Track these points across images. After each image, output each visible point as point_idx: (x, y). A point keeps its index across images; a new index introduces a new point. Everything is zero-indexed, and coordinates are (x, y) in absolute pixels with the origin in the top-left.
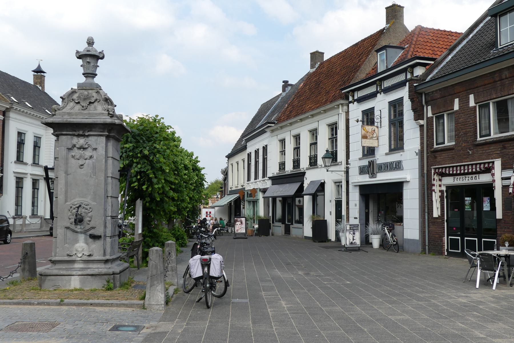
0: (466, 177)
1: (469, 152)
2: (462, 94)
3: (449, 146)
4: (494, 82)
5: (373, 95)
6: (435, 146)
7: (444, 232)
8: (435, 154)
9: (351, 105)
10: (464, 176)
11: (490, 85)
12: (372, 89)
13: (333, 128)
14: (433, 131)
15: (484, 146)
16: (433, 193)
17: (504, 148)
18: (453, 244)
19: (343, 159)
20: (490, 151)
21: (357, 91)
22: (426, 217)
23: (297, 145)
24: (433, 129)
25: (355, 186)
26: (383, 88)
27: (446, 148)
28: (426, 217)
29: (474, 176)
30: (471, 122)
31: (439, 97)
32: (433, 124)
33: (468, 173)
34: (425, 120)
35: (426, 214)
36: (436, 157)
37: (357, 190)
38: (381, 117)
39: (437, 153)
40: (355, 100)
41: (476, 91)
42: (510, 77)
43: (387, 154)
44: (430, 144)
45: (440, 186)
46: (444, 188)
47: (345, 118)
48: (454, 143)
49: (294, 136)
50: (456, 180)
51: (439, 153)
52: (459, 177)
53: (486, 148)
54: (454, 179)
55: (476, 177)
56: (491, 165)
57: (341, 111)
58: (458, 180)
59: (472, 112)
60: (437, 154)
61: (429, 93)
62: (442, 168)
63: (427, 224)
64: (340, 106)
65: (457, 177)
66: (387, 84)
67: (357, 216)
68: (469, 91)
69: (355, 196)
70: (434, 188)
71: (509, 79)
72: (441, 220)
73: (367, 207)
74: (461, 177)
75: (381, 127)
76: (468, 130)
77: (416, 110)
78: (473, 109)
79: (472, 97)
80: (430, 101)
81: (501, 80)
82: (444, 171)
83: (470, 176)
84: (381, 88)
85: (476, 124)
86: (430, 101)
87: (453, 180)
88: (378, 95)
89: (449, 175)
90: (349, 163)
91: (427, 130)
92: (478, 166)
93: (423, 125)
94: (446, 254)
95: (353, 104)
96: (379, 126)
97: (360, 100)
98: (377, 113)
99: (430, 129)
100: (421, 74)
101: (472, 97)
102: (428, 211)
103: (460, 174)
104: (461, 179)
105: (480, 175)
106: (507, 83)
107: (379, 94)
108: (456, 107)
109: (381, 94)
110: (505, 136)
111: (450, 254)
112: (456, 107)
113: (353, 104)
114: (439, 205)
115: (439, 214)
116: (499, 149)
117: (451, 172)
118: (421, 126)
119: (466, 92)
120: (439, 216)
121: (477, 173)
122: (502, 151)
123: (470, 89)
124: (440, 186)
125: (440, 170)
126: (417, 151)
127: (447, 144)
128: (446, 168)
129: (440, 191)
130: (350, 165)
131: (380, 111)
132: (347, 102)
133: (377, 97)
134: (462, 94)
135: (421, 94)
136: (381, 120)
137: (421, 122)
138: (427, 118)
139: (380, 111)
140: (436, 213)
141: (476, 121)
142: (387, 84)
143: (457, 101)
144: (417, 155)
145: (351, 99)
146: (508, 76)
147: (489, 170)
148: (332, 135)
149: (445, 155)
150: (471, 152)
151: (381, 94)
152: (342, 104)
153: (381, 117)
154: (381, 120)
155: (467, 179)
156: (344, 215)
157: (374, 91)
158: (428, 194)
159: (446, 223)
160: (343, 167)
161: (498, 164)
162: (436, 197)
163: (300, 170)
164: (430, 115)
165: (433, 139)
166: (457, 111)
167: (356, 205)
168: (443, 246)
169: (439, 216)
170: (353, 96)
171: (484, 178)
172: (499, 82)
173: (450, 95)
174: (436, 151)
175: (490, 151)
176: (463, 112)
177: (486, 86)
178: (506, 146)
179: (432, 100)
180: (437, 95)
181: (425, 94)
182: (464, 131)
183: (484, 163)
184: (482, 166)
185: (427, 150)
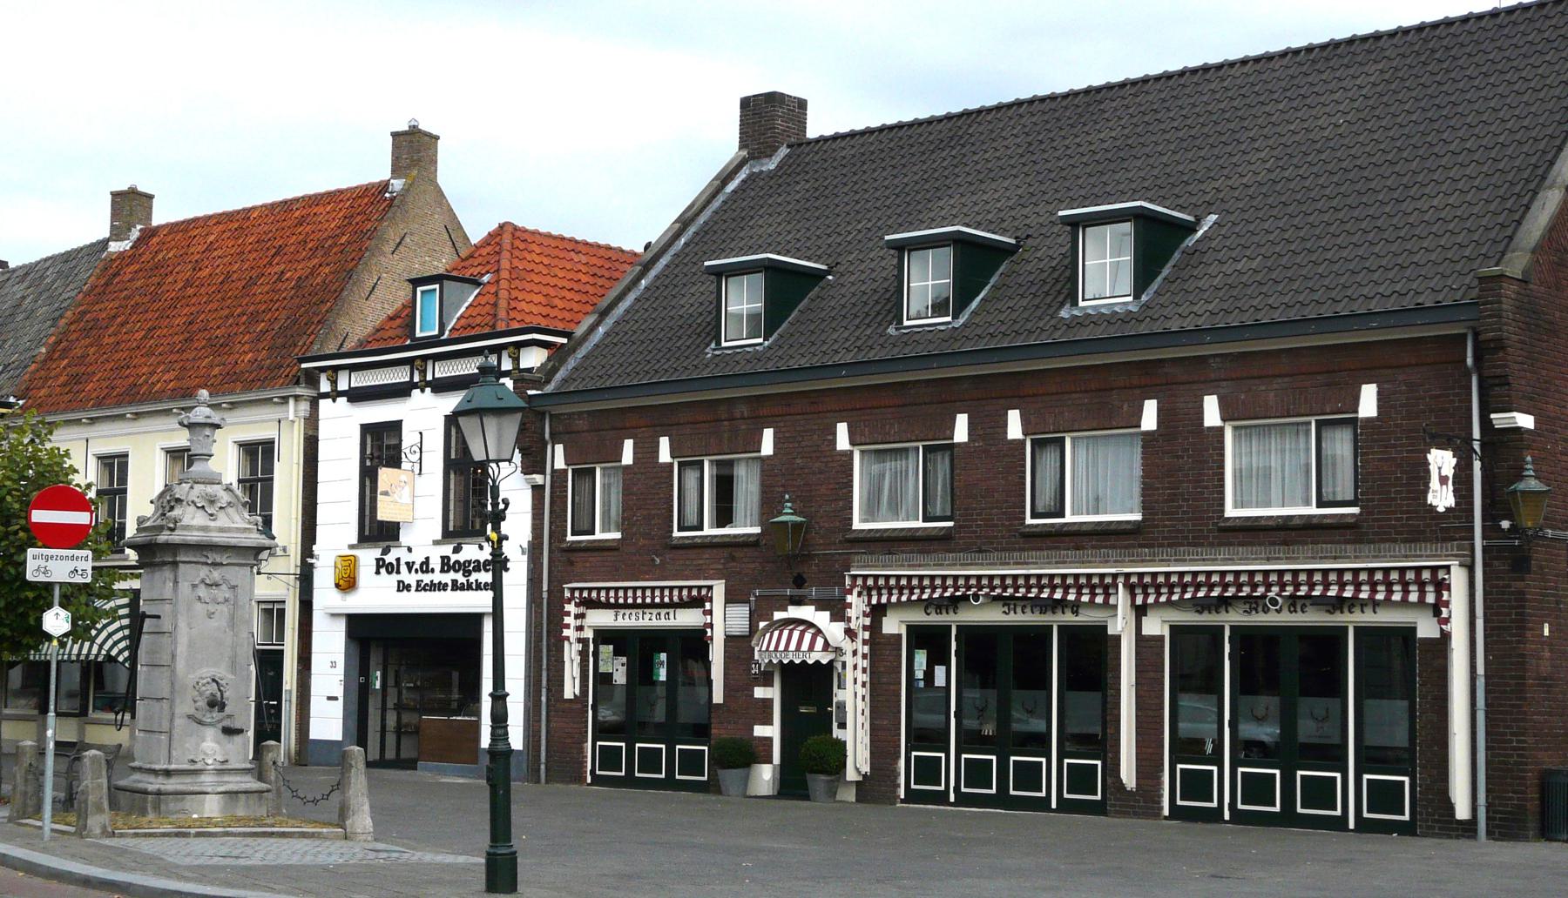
0: (644, 613)
1: (653, 560)
2: (643, 432)
3: (607, 540)
4: (715, 421)
5: (400, 392)
6: (570, 538)
7: (587, 732)
8: (570, 555)
9: (324, 404)
10: (640, 611)
11: (707, 425)
12: (400, 376)
13: (259, 454)
14: (566, 502)
15: (690, 552)
16: (566, 643)
17: (733, 559)
18: (609, 758)
19: (293, 541)
20: (701, 562)
21: (348, 371)
22: (544, 699)
23: (111, 483)
24: (566, 496)
25: (333, 615)
26: (429, 378)
27: (596, 544)
28: (544, 699)
29: (663, 612)
30: (662, 496)
31: (585, 428)
32: (567, 487)
33: (653, 605)
34: (548, 477)
35: (544, 691)
36: (571, 563)
37: (340, 627)
38: (421, 449)
39: (576, 554)
40: (342, 394)
41: (674, 432)
42: (748, 418)
43: (436, 543)
44: (558, 533)
45: (580, 628)
46: (589, 634)
47: (302, 432)
48: (618, 535)
49: (100, 458)
50: (620, 618)
51: (582, 554)
52: (628, 612)
53: (692, 554)
54: (616, 616)
55: (668, 614)
56: (704, 592)
57: (295, 412)
58: (626, 617)
59: (664, 475)
60: (574, 557)
61: (561, 414)
62: (590, 590)
63: (544, 713)
64: (291, 402)
65: (622, 611)
66: (442, 371)
67: (339, 691)
68: (658, 429)
69: (330, 644)
70: (566, 633)
71: (749, 421)
72: (579, 706)
73: (364, 670)
74: (634, 611)
75: (420, 474)
76: (653, 512)
77: (525, 452)
78: (668, 469)
79: (664, 443)
80: (560, 433)
81: (732, 419)
82: (594, 594)
83: (655, 611)
84: (425, 376)
85: (672, 501)
86: (560, 433)
87: (614, 618)
88: (416, 392)
89: (607, 606)
90: (316, 553)
91: (551, 497)
92: (676, 592)
93: (542, 487)
94: (589, 780)
95: (334, 401)
96: (417, 471)
97: (357, 396)
98: (408, 439)
99: (558, 497)
100: (539, 365)
101: (664, 443)
102: (548, 684)
103: (634, 606)
104: (633, 617)
105: (678, 611)
106: (743, 427)
107: (418, 390)
108: (628, 457)
109: (423, 391)
110: (735, 536)
111: (597, 780)
112: (628, 457)
113: (334, 401)
114: (577, 672)
115: (577, 692)
116: (722, 561)
117: (621, 601)
118: (537, 490)
119: (651, 429)
120: (575, 695)
121: (673, 605)
122: (727, 566)
123: (661, 426)
124: (580, 628)
125: (585, 594)
126: (525, 546)
127: (599, 535)
128: (599, 589)
129: (579, 640)
130: (317, 559)
131: (421, 433)
132: (313, 393)
133: (410, 396)
134: (643, 432)
135: (543, 414)
136: (421, 459)
137: (538, 479)
138: (553, 471)
139: (421, 433)
140: (570, 690)
141: (672, 496)
142: (442, 371)
143: (628, 445)
144: (523, 553)
145: (325, 386)
146: (746, 415)
147: (697, 602)
148: (254, 471)
149: (594, 558)
150: (658, 561)
151: (423, 391)
152: (297, 398)
153: (421, 449)
154: (421, 459)
155: (647, 617)
156: (290, 691)
157: (402, 380)
158: (548, 645)
159: (590, 712)
160: (292, 563)
161: (719, 589)
162: (571, 653)
163: (126, 560)
164: (560, 463)
165: (566, 521)
166: (627, 467)
167: (333, 665)
168: (583, 763)
169: (575, 695)
170: (334, 382)
171: (688, 618)
172: (726, 423)
173: (614, 429)
174: (575, 549)
175: (701, 562)
176: (642, 471)
177: (698, 426)
178: (737, 555)
179: (568, 433)
180: (581, 424)
181: (551, 416)
182: (645, 512)
183: (690, 588)
184: (685, 592)
185: (550, 543)
